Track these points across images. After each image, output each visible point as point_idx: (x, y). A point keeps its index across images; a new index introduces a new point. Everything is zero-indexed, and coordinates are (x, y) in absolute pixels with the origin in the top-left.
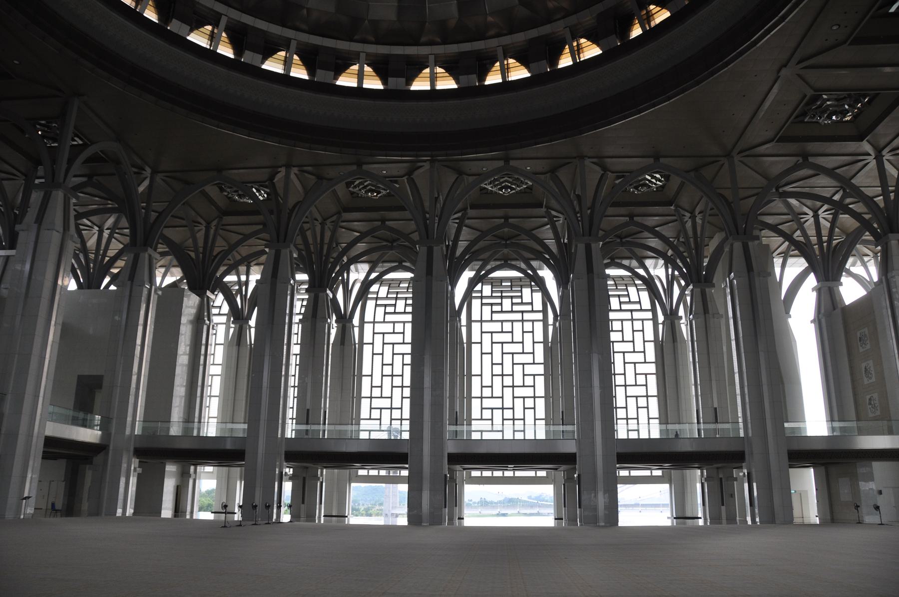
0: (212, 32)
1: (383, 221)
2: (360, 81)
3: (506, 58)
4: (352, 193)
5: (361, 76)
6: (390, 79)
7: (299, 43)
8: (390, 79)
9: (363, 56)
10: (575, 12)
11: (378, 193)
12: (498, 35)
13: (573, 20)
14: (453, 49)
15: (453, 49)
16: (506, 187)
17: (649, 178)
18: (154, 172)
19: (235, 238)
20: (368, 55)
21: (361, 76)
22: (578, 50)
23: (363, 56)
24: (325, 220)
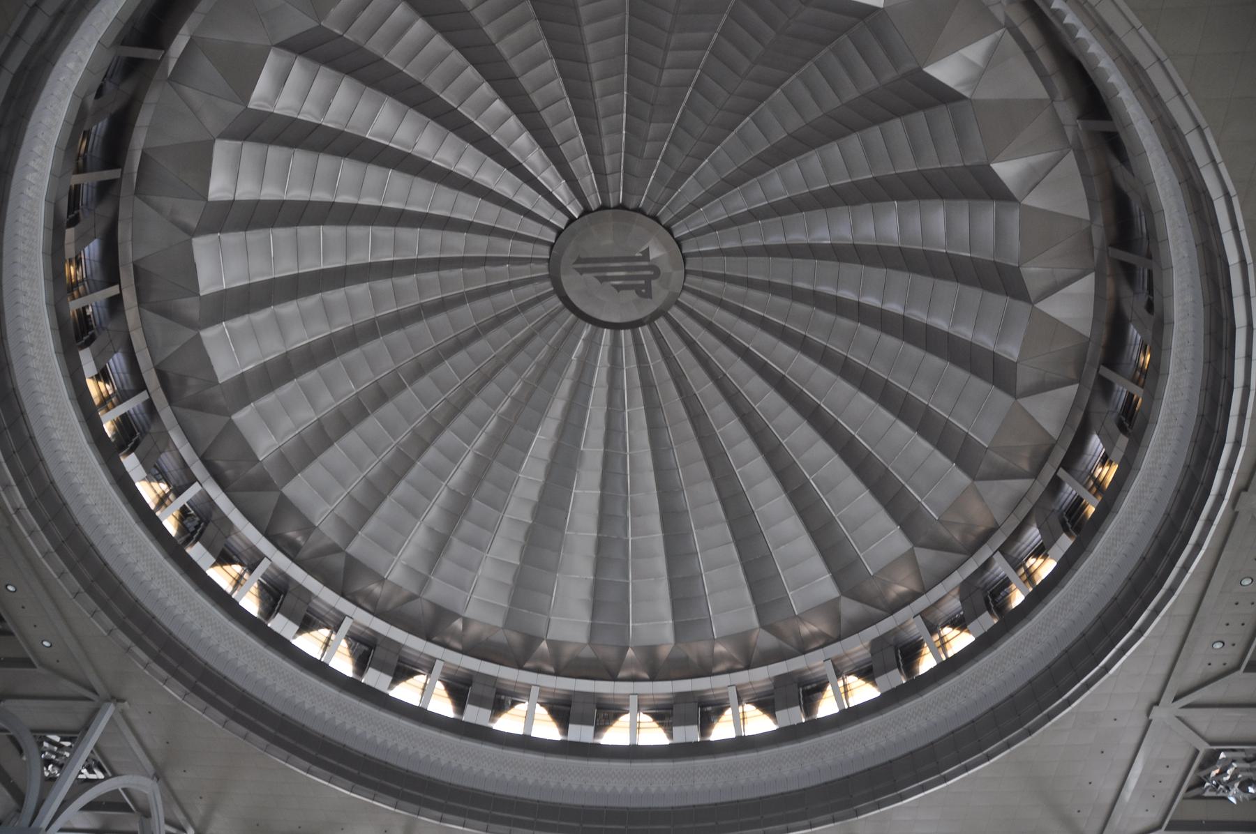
10: (839, 639)
13: (835, 649)
22: (846, 692)
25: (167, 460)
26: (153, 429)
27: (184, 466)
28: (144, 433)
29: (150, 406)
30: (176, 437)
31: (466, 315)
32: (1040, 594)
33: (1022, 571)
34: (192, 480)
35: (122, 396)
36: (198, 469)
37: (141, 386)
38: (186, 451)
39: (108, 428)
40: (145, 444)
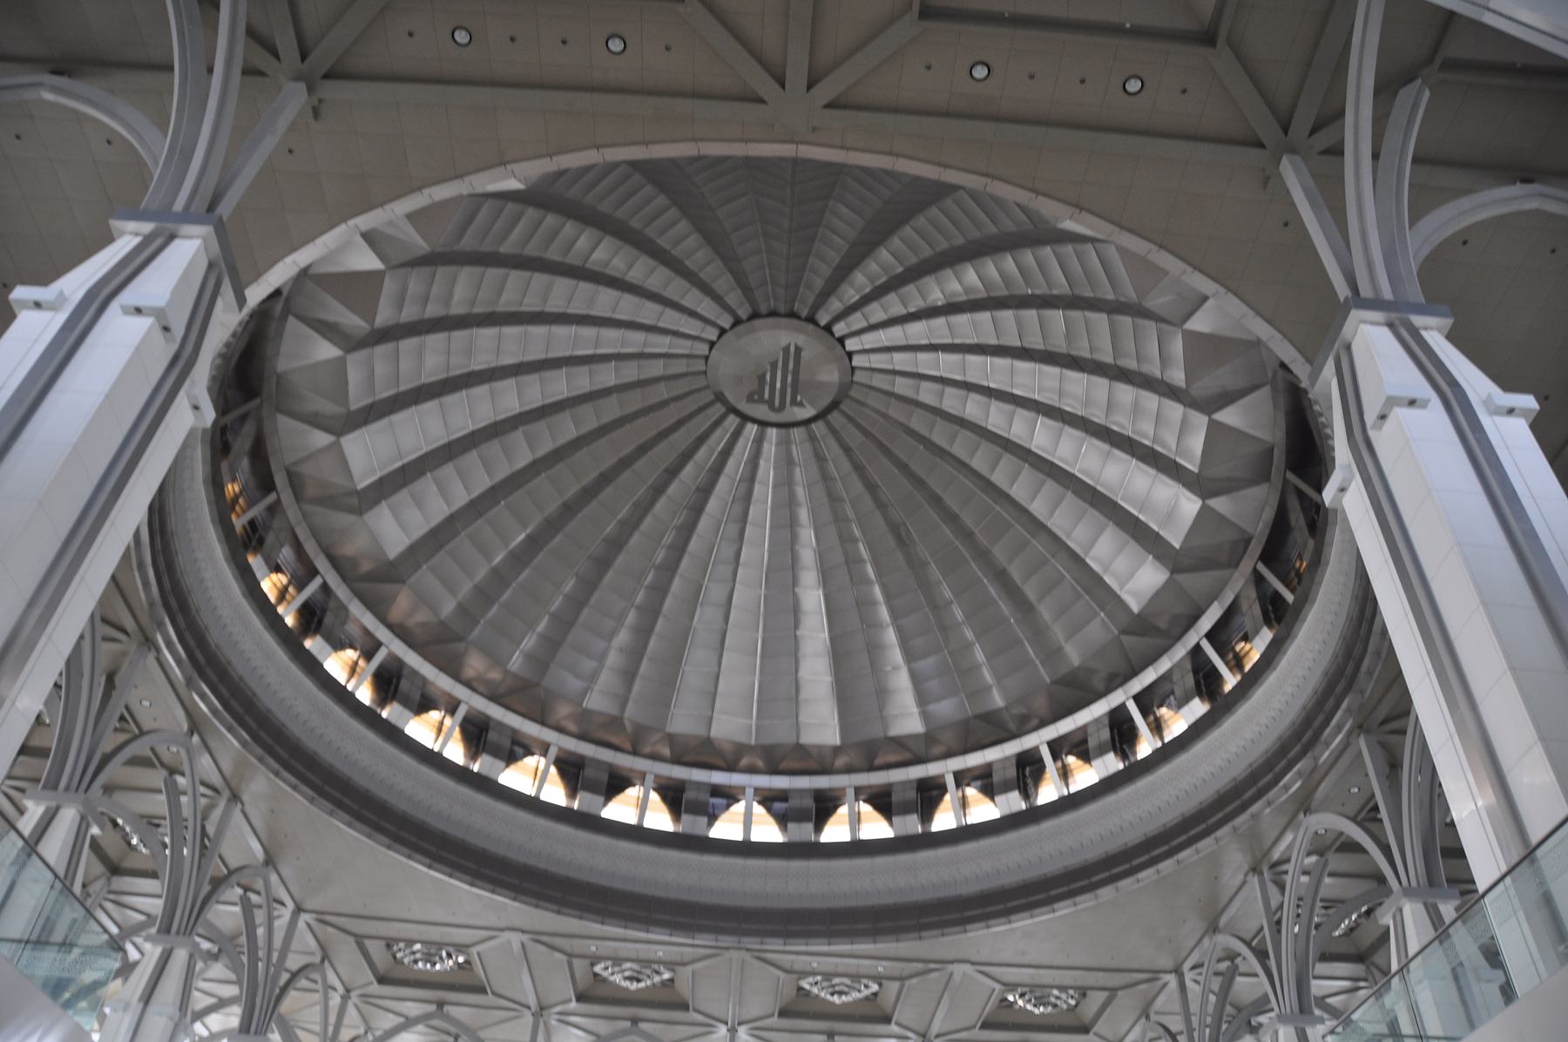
0: (442, 723)
1: (635, 1021)
2: (642, 816)
3: (857, 800)
4: (596, 975)
5: (643, 806)
6: (685, 817)
7: (560, 749)
8: (685, 817)
9: (650, 779)
11: (639, 981)
12: (849, 770)
14: (780, 782)
15: (780, 782)
16: (840, 993)
17: (1056, 992)
18: (299, 909)
19: (390, 1021)
20: (656, 776)
21: (643, 806)
23: (650, 779)
24: (542, 1009)
25: (351, 628)
26: (332, 605)
27: (366, 632)
28: (324, 611)
29: (325, 587)
30: (356, 609)
31: (627, 440)
32: (1250, 681)
33: (1231, 656)
34: (379, 644)
35: (300, 583)
36: (382, 633)
37: (314, 572)
38: (369, 621)
39: (290, 621)
40: (328, 620)
